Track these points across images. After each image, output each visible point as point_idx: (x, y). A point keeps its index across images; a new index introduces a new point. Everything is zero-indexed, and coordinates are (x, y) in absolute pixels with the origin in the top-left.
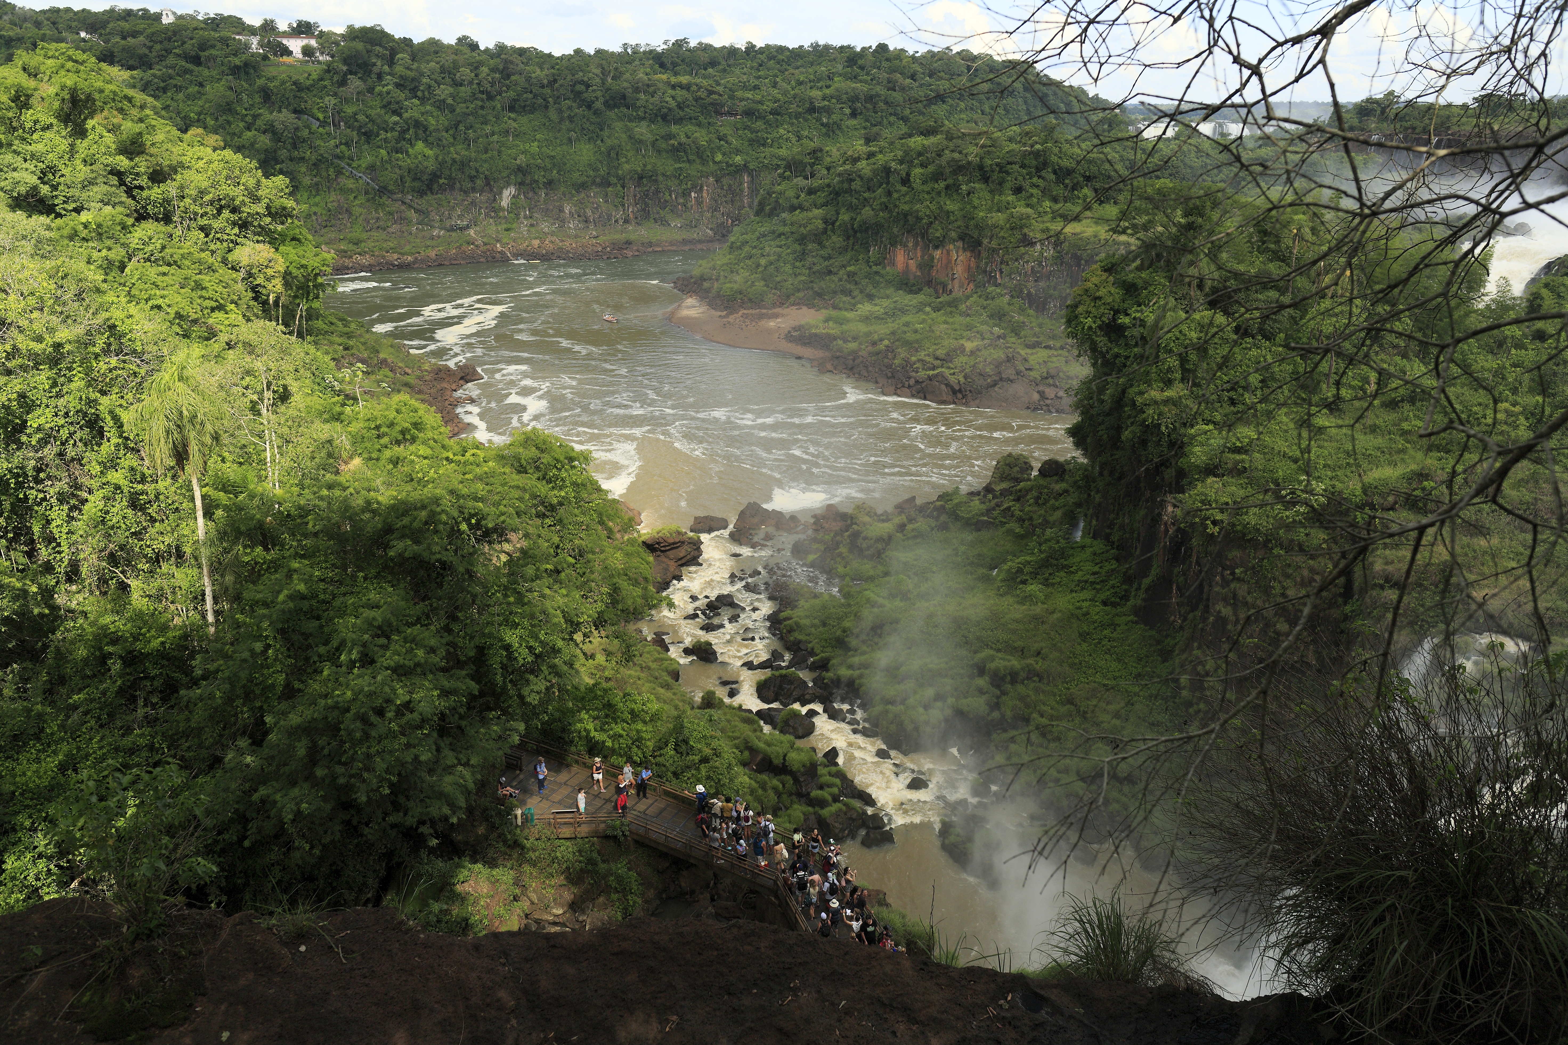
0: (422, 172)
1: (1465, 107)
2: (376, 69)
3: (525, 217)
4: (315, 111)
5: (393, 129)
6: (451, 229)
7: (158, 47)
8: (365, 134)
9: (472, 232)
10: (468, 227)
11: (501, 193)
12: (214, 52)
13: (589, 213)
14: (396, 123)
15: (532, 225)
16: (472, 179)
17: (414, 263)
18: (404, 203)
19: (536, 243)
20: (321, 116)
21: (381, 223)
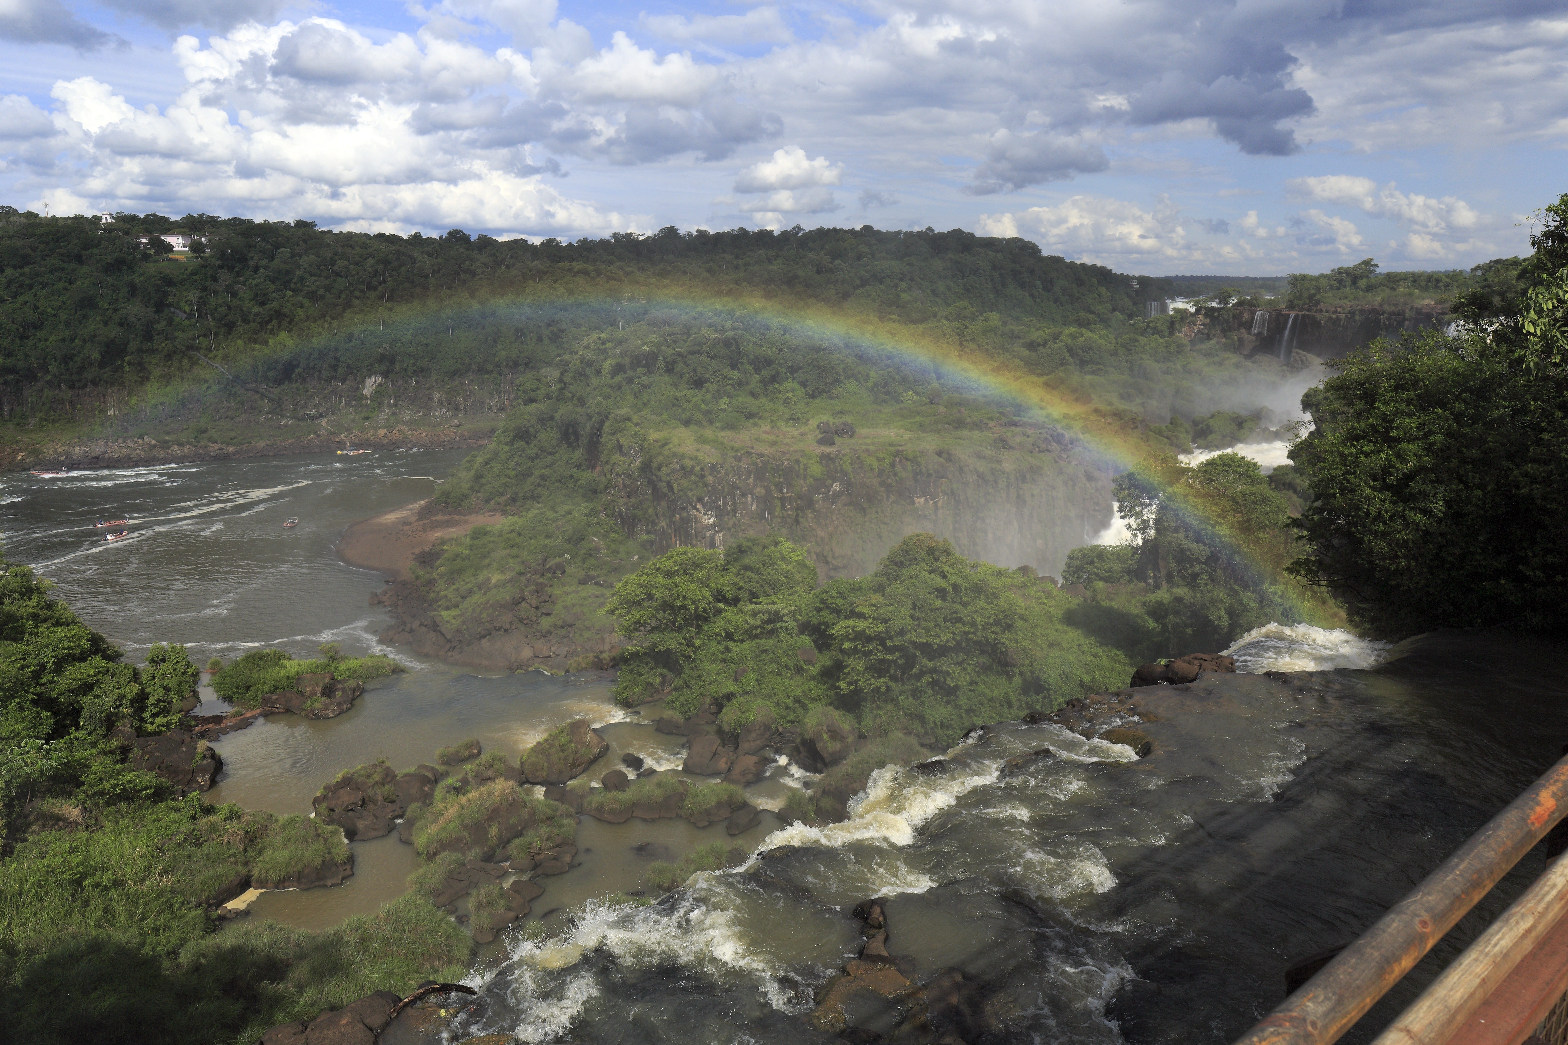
0: (276, 362)
1: (288, 225)
2: (252, 263)
3: (389, 406)
4: (182, 304)
5: (254, 321)
6: (303, 419)
7: (42, 246)
8: (226, 325)
9: (324, 421)
10: (321, 416)
11: (363, 381)
12: (94, 251)
13: (460, 400)
14: (257, 314)
15: (394, 414)
16: (334, 368)
17: (235, 454)
18: (257, 392)
19: (382, 432)
20: (187, 309)
21: (230, 413)
